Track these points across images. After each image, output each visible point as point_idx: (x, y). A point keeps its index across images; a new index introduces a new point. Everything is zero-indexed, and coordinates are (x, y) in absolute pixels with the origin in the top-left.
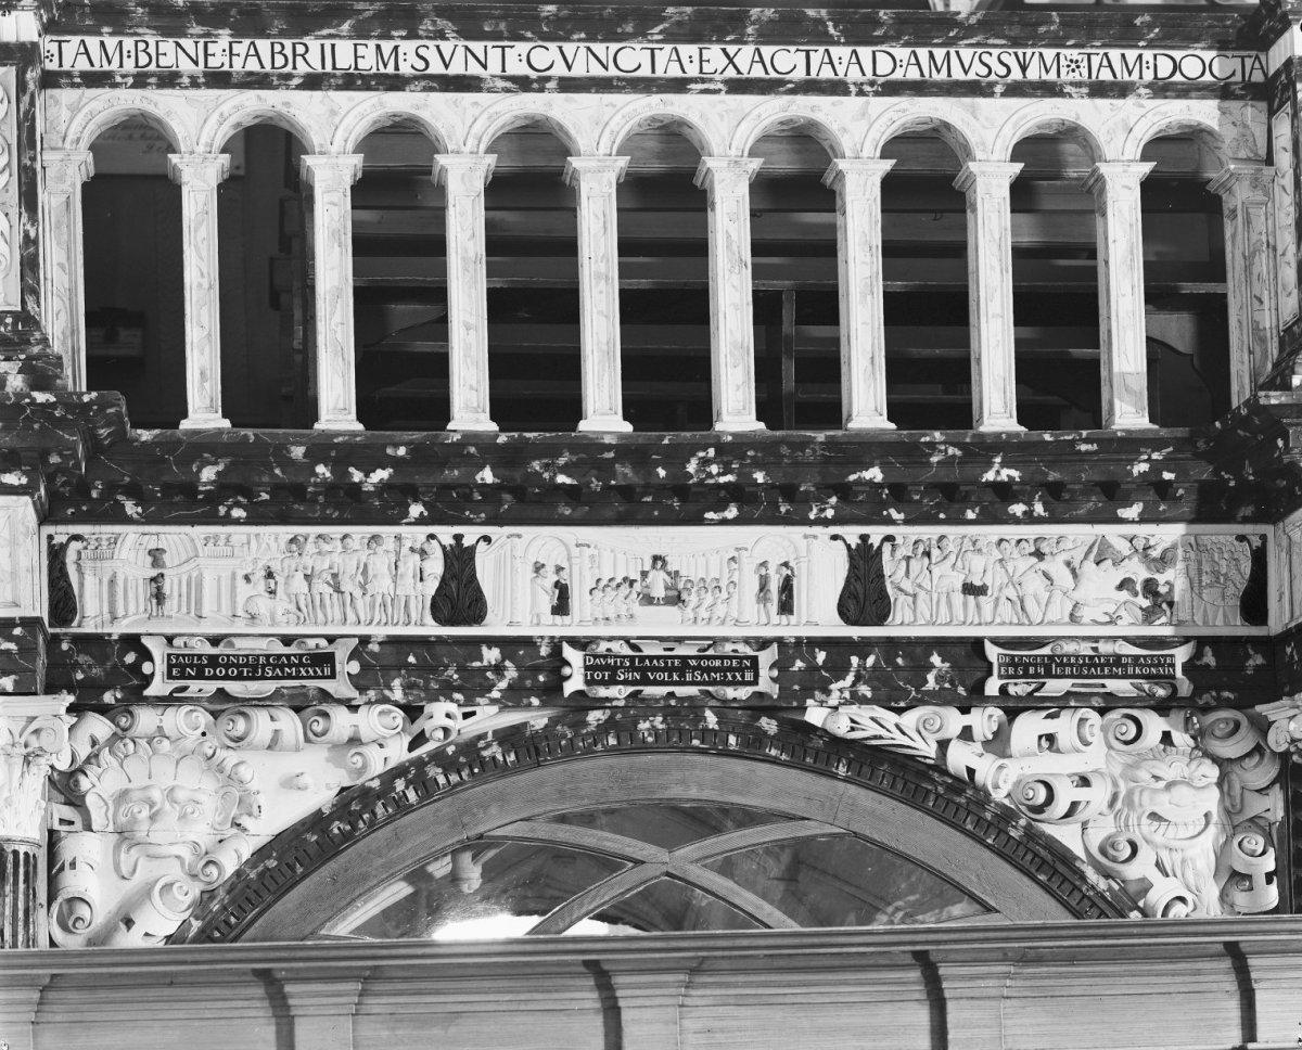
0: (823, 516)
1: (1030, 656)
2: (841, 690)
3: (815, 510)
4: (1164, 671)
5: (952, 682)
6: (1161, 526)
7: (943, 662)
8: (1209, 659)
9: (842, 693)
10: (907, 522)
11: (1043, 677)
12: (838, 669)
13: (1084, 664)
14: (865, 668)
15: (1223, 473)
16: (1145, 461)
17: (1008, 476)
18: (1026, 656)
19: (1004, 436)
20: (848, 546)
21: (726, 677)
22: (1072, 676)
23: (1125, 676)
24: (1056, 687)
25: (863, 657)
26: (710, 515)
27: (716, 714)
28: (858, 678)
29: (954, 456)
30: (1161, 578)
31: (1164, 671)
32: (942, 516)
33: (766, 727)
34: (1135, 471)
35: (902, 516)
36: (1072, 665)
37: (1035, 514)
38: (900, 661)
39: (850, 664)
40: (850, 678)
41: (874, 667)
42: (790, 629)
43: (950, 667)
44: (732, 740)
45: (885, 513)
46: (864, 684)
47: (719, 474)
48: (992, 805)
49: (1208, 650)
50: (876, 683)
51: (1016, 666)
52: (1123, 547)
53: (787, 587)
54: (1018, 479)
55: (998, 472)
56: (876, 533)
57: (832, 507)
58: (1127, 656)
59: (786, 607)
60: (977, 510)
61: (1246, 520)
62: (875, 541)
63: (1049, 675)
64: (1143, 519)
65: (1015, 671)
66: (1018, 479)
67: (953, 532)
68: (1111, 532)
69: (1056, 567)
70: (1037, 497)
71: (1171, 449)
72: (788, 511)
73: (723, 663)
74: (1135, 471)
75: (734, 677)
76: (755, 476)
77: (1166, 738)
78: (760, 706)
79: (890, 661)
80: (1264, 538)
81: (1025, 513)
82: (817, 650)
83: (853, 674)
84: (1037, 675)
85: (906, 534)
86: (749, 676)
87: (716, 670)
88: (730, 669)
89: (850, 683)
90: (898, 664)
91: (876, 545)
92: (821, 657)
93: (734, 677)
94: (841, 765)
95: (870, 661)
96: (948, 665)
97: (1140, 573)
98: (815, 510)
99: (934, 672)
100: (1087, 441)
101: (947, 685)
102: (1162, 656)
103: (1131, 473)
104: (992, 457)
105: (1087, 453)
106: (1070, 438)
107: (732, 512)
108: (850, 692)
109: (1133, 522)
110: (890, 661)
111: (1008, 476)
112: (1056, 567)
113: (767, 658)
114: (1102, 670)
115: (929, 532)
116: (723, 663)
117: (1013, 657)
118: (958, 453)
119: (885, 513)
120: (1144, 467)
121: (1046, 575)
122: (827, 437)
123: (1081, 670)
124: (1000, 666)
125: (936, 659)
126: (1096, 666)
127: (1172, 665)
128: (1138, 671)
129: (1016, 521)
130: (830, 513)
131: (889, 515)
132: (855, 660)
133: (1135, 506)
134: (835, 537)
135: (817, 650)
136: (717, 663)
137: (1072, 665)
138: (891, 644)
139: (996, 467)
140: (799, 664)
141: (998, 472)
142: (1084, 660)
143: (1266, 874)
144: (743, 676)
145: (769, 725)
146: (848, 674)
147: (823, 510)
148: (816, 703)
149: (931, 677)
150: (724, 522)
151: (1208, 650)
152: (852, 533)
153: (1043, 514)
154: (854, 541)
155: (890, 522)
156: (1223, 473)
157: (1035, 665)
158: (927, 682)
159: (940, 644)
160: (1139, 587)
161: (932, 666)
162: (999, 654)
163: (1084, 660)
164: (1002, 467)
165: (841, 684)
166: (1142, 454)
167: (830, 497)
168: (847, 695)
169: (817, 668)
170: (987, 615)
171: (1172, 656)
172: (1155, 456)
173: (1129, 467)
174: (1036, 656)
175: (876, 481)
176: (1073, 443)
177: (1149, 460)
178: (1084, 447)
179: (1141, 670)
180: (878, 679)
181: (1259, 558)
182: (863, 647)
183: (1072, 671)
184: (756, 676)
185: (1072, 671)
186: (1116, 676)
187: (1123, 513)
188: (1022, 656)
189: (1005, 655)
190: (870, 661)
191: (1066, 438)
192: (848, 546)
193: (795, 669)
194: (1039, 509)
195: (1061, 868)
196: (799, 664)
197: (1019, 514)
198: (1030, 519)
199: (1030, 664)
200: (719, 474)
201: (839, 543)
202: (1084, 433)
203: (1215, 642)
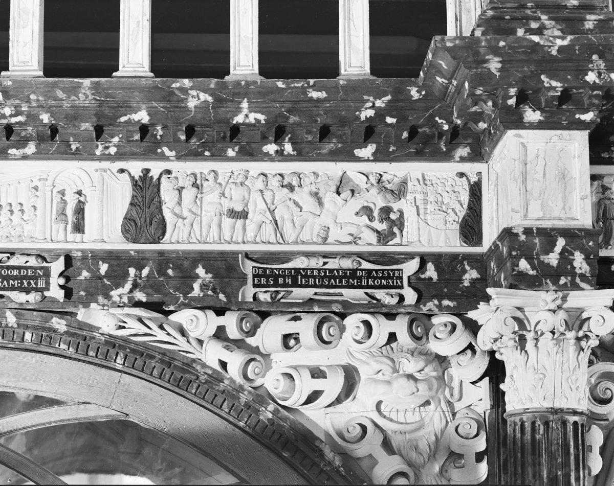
0: (107, 152)
1: (280, 269)
2: (120, 296)
3: (100, 148)
4: (393, 282)
5: (214, 290)
6: (393, 164)
7: (207, 273)
8: (431, 272)
9: (121, 298)
10: (179, 158)
11: (290, 286)
12: (118, 278)
13: (325, 276)
14: (141, 278)
15: (437, 119)
16: (370, 108)
17: (255, 119)
18: (276, 269)
19: (243, 83)
20: (133, 178)
21: (22, 283)
22: (315, 286)
23: (360, 287)
24: (301, 294)
25: (140, 268)
26: (12, 151)
27: (15, 315)
28: (135, 286)
29: (206, 102)
30: (396, 206)
31: (393, 282)
32: (207, 153)
33: (57, 326)
34: (363, 117)
35: (174, 153)
36: (314, 277)
37: (285, 153)
38: (170, 272)
39: (128, 274)
40: (128, 286)
41: (148, 276)
42: (76, 244)
43: (212, 278)
44: (28, 336)
45: (159, 151)
46: (140, 291)
47: (12, 116)
48: (246, 393)
49: (430, 266)
50: (150, 290)
51: (267, 277)
52: (360, 181)
53: (80, 211)
54: (263, 122)
55: (247, 116)
56: (156, 168)
57: (115, 146)
58: (362, 270)
59: (79, 227)
60: (237, 149)
61: (463, 159)
62: (155, 173)
63: (295, 284)
64: (378, 157)
65: (267, 281)
66: (263, 122)
67: (223, 168)
68: (351, 169)
69: (303, 196)
70: (287, 138)
71: (389, 97)
72: (77, 148)
73: (20, 272)
74: (363, 117)
75: (29, 284)
76: (41, 117)
77: (392, 337)
78: (48, 309)
79: (162, 272)
80: (479, 174)
81: (277, 152)
82: (101, 263)
83: (131, 282)
84: (285, 285)
85: (183, 169)
86: (41, 284)
87: (14, 278)
88: (26, 277)
89: (128, 290)
90: (168, 274)
91: (156, 177)
92: (104, 268)
93: (29, 284)
94: (119, 358)
95: (145, 272)
96: (210, 275)
97: (378, 201)
98: (100, 148)
99: (200, 281)
100: (315, 88)
101: (210, 293)
102: (392, 270)
103: (358, 118)
104: (240, 103)
105: (319, 100)
106: (300, 85)
107: (31, 148)
108: (129, 297)
109: (368, 160)
110: (162, 272)
111: (255, 119)
112: (303, 196)
113: (57, 267)
114: (341, 281)
115: (202, 167)
116: (20, 272)
117: (265, 269)
118: (210, 99)
119: (159, 151)
120: (370, 113)
121: (296, 203)
122: (92, 83)
123: (323, 281)
124: (254, 276)
125: (200, 271)
126: (335, 278)
127: (401, 278)
128: (370, 282)
129: (267, 157)
130: (113, 150)
131: (163, 152)
132: (132, 271)
133: (369, 147)
134: (122, 171)
135: (101, 263)
136: (16, 272)
137: (314, 277)
138: (163, 260)
139: (245, 111)
140: (85, 274)
141: (247, 116)
142: (325, 273)
143: (476, 453)
144: (36, 284)
145: (59, 324)
146: (126, 283)
147: (107, 148)
148: (99, 307)
149: (196, 286)
150: (25, 157)
151: (430, 266)
152: (136, 167)
153: (292, 153)
154: (137, 174)
155: (163, 157)
156: (437, 119)
157: (284, 277)
158: (192, 289)
159: (204, 258)
160: (376, 214)
161: (197, 277)
162: (253, 267)
163: (325, 273)
164: (251, 112)
165: (120, 291)
166: (365, 101)
167: (112, 137)
168: (125, 300)
169: (100, 278)
170: (250, 236)
171: (399, 270)
172: (378, 103)
173: (357, 113)
174: (285, 269)
175: (143, 122)
176: (304, 90)
177: (373, 107)
178: (315, 95)
179: (374, 282)
180: (152, 287)
181: (476, 191)
182: (139, 262)
183: (315, 282)
184: (48, 284)
185: (315, 282)
186: (352, 287)
187: (359, 152)
188: (273, 269)
189: (259, 268)
190: (145, 272)
191: (296, 85)
192: (133, 178)
193: (82, 278)
194: (288, 148)
195: (302, 447)
196: (85, 274)
197: (272, 152)
198: (281, 156)
199: (279, 276)
200: (12, 116)
201: (125, 175)
202: (312, 81)
203: (437, 258)
